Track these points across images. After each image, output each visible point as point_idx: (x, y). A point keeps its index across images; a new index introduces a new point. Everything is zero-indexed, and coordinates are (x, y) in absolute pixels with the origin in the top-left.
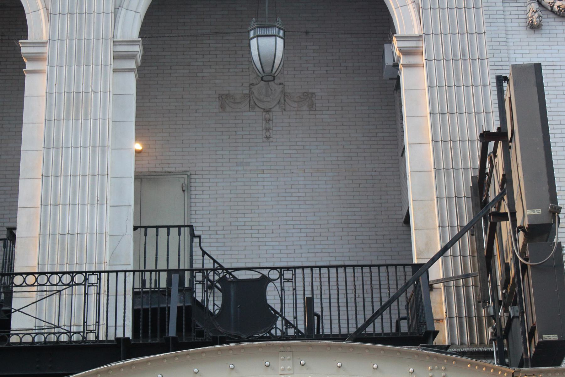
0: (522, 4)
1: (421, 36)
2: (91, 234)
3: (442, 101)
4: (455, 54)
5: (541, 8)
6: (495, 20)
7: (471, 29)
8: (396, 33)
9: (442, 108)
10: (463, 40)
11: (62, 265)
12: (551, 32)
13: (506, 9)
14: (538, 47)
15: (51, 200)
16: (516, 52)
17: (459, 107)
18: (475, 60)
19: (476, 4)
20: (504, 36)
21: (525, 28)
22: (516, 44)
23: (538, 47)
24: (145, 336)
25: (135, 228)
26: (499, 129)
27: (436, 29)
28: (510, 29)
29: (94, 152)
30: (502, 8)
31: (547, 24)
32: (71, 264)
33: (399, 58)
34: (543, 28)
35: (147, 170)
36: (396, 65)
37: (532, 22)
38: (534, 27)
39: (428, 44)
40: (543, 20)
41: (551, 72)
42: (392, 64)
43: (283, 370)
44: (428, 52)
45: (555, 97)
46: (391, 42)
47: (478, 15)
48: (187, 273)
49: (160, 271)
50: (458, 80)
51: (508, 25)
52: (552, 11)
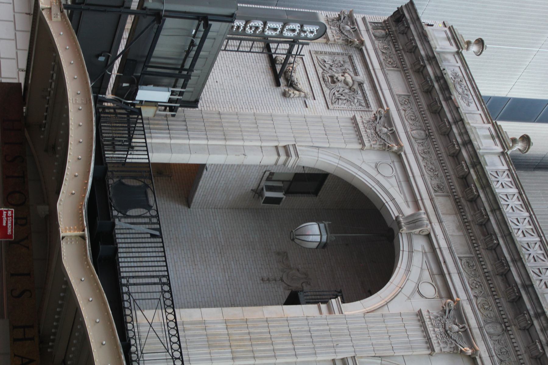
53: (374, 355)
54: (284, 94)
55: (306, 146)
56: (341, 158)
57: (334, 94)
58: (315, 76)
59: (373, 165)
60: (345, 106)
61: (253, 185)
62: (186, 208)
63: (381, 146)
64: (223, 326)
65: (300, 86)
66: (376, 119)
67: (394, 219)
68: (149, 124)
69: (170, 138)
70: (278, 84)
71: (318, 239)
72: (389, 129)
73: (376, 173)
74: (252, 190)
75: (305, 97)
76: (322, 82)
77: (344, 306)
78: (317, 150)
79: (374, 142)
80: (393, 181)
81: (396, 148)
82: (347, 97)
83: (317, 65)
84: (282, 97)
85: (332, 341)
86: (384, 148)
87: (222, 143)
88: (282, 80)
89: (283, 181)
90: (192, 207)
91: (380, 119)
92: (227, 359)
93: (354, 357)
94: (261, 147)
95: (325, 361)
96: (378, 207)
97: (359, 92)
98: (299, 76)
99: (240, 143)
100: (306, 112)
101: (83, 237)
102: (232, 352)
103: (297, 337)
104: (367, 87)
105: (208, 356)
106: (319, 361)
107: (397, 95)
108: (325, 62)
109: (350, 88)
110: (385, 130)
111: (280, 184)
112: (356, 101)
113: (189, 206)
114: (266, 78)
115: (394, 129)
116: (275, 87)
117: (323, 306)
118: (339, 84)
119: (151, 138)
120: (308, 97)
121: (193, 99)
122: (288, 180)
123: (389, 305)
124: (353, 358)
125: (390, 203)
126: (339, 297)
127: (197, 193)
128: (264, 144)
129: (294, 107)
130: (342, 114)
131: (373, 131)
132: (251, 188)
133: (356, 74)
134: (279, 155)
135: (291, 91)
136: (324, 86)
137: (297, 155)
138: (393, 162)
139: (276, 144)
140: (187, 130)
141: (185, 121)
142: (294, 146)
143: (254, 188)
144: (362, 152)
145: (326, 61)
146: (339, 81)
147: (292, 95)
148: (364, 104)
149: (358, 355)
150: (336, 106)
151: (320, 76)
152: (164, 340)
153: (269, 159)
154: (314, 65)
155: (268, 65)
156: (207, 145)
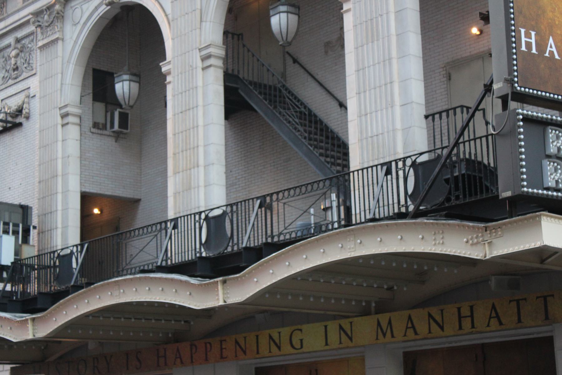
2: (388, 132)
11: (389, 156)
15: (363, 113)
24: (470, 195)
25: (426, 117)
29: (384, 65)
32: (383, 158)
35: (469, 54)
43: (350, 249)
48: (393, 164)
49: (481, 138)
53: (198, 31)
54: (27, 118)
55: (61, 97)
56: (69, 62)
57: (26, 68)
58: (14, 87)
59: (74, 27)
60: (34, 56)
61: (109, 143)
62: (141, 203)
63: (59, 20)
64: (177, 175)
65: (20, 103)
66: (40, 26)
67: (109, 7)
68: (48, 249)
69: (56, 228)
70: (20, 125)
71: (126, 84)
72: (45, 13)
73: (79, 25)
74: (116, 141)
75: (28, 97)
76: (18, 80)
77: (168, 60)
78: (64, 86)
79: (56, 27)
80: (85, 7)
81: (57, 7)
82: (28, 54)
83: (6, 85)
84: (30, 119)
85: (189, 71)
86: (61, 17)
87: (60, 179)
88: (18, 120)
89: (106, 112)
90: (139, 198)
91: (39, 22)
92: (198, 172)
93: (199, 49)
94: (63, 141)
95: (203, 78)
96: (106, 22)
97: (23, 42)
98: (13, 104)
99: (60, 162)
100: (38, 95)
101: (33, 320)
102: (194, 168)
103: (186, 105)
104: (20, 34)
105: (196, 189)
106: (203, 83)
107: (23, 3)
108: (4, 77)
109: (21, 51)
110: (46, 17)
111: (109, 115)
112: (30, 46)
113: (138, 201)
114: (17, 134)
115: (44, 8)
116: (23, 127)
117: (169, 79)
118: (19, 63)
119: (56, 246)
120: (28, 94)
121: (20, 210)
122: (104, 107)
123: (167, 14)
124: (200, 50)
125: (100, 10)
126: (161, 64)
127: (121, 195)
128: (60, 138)
129: (35, 107)
130: (38, 58)
131: (48, 29)
132: (114, 143)
133: (9, 46)
134: (67, 124)
135: (24, 112)
136: (20, 78)
137: (66, 106)
138: (71, 7)
139: (59, 127)
140: (51, 213)
141: (45, 215)
142: (60, 109)
143: (114, 140)
144: (65, 39)
145: (3, 75)
146: (16, 63)
147: (27, 111)
148: (32, 37)
149: (198, 45)
150: (34, 67)
151: (13, 82)
152: (148, 239)
153: (74, 132)
154: (6, 88)
155: (8, 134)
156: (62, 193)
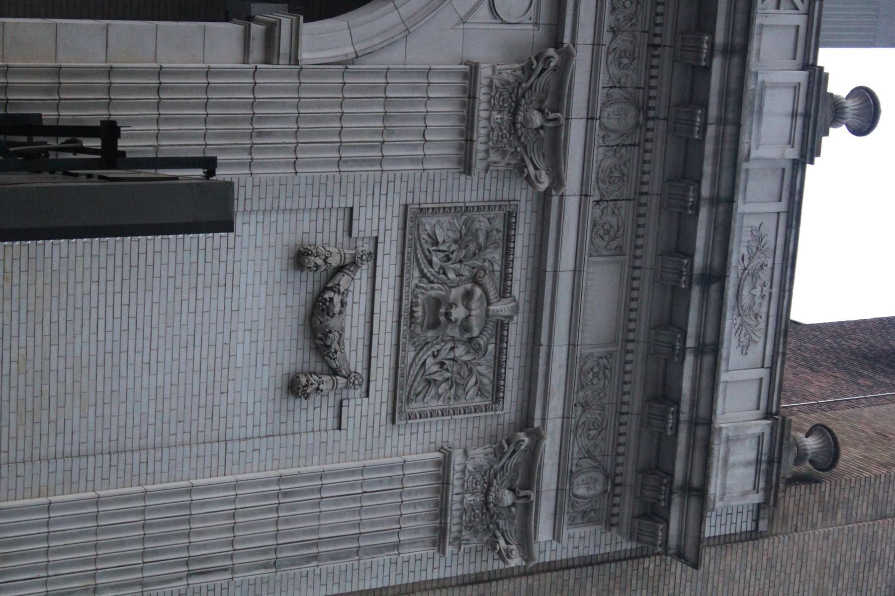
0: (340, 240)
1: (297, 62)
3: (181, 89)
4: (263, 119)
5: (330, 271)
6: (316, 193)
7: (304, 151)
8: (306, 21)
9: (171, 89)
10: (285, 134)
12: (290, 286)
13: (334, 213)
14: (265, 263)
16: (260, 225)
17: (168, 120)
18: (250, 154)
19: (346, 162)
20: (288, 207)
21: (299, 242)
22: (273, 225)
23: (265, 263)
26: (123, 153)
27: (307, 90)
28: (300, 217)
30: (336, 205)
31: (304, 279)
33: (259, 22)
34: (298, 273)
36: (250, 19)
37: (308, 254)
38: (300, 258)
39: (282, 75)
40: (311, 274)
41: (222, 282)
42: (252, 14)
44: (269, 74)
45: (178, 285)
46: (291, 11)
47: (326, 162)
50: (217, 121)
51: (307, 215)
52: (325, 289)
